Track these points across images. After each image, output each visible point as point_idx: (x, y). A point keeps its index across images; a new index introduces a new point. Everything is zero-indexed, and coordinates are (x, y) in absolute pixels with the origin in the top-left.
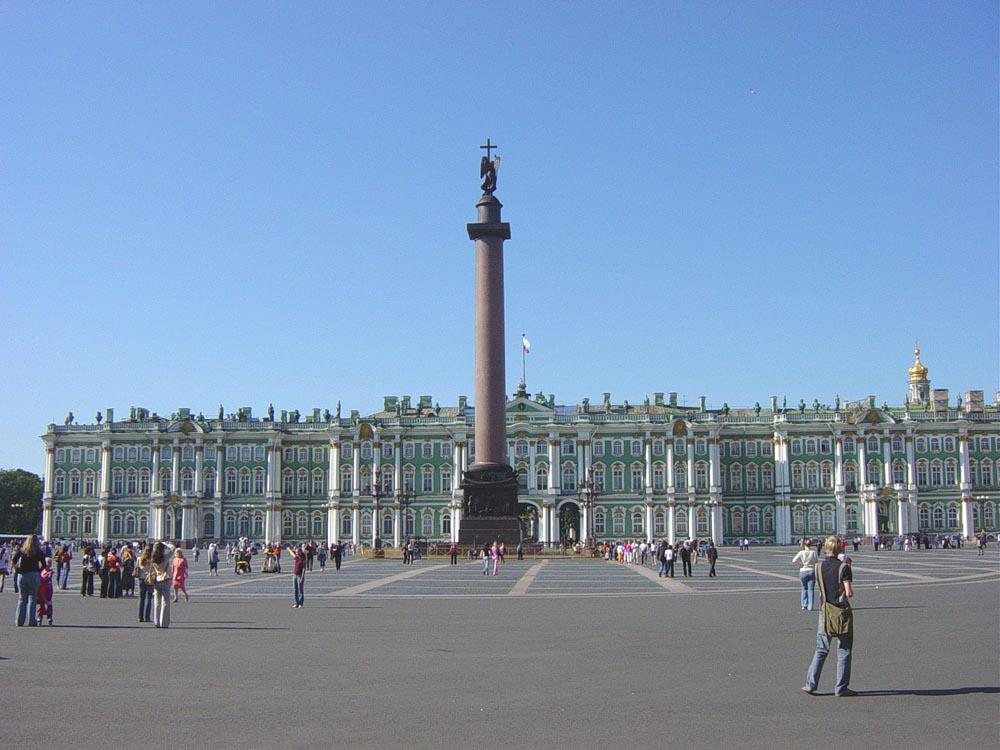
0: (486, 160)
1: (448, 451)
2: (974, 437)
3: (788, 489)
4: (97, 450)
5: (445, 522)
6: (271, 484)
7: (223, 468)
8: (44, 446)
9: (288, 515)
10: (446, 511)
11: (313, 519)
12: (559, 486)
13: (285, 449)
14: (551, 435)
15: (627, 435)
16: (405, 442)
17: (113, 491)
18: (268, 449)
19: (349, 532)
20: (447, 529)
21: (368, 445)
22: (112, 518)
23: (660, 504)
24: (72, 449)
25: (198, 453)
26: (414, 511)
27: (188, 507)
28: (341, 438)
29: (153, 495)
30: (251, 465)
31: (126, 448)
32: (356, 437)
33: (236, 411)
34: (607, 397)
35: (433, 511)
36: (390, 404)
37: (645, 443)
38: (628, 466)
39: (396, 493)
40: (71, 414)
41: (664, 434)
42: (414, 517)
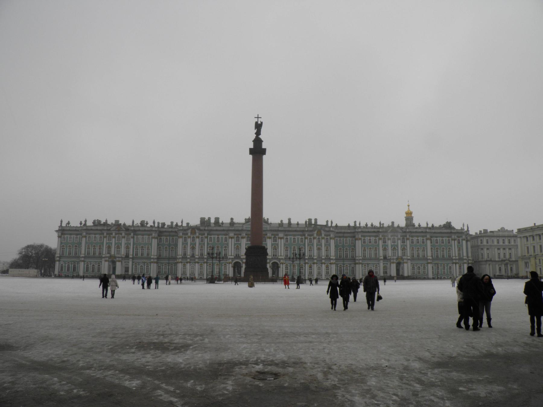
0: (256, 123)
1: (226, 240)
2: (432, 239)
3: (361, 258)
6: (154, 252)
7: (133, 245)
8: (56, 235)
10: (225, 264)
15: (299, 235)
16: (209, 236)
21: (193, 237)
24: (69, 236)
27: (119, 261)
29: (103, 256)
33: (139, 222)
34: (289, 220)
36: (202, 220)
37: (305, 238)
41: (313, 235)
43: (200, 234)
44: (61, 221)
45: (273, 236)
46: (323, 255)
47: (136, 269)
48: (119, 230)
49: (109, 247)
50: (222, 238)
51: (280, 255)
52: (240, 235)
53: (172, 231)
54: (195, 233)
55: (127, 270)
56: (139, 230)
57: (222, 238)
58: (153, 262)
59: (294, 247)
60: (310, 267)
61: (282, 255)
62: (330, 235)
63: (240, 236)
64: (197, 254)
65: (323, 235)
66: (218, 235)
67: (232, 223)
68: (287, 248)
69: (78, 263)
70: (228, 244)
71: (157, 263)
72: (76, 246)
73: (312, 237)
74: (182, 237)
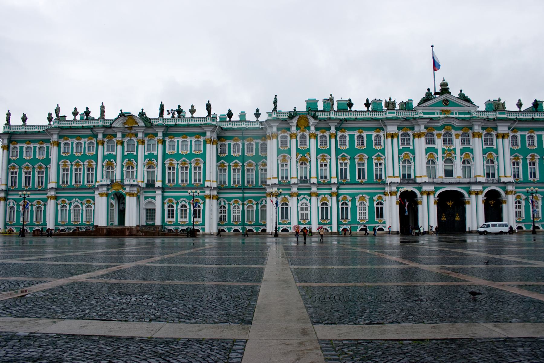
4: (48, 147)
5: (378, 208)
9: (222, 203)
11: (246, 207)
13: (219, 143)
16: (339, 134)
17: (61, 182)
18: (205, 142)
19: (287, 218)
20: (380, 213)
21: (303, 136)
22: (59, 207)
24: (25, 146)
25: (140, 146)
27: (131, 194)
28: (278, 129)
29: (97, 184)
30: (191, 156)
31: (72, 143)
32: (294, 129)
36: (312, 104)
40: (24, 115)
42: (350, 204)
43: (317, 129)
44: (8, 115)
45: (484, 132)
47: (171, 214)
48: (131, 128)
49: (110, 166)
50: (369, 137)
51: (502, 174)
52: (412, 128)
53: (247, 129)
54: (308, 127)
55: (150, 213)
56: (176, 126)
57: (369, 137)
58: (210, 197)
61: (508, 174)
63: (410, 133)
64: (314, 174)
68: (516, 158)
69: (45, 201)
70: (383, 151)
71: (218, 199)
72: (40, 167)
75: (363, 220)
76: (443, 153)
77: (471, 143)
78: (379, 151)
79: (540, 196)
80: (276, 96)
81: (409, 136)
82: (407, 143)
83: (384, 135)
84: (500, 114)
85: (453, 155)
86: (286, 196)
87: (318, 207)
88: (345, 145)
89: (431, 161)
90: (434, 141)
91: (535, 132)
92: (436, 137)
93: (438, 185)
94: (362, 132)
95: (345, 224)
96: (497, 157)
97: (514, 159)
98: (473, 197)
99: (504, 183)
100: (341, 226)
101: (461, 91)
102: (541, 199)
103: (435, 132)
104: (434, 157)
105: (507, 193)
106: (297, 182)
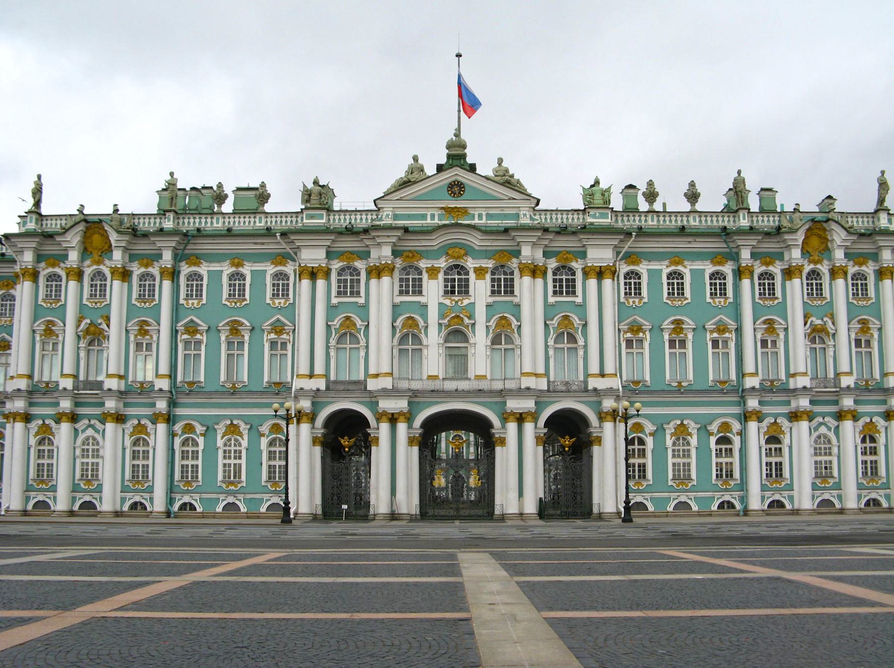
12: (541, 370)
14: (526, 251)
16: (185, 269)
21: (99, 274)
23: (776, 416)
26: (199, 429)
28: (39, 258)
32: (73, 257)
35: (244, 428)
37: (739, 273)
38: (701, 329)
39: (163, 384)
41: (780, 256)
42: (201, 441)
45: (553, 264)
46: (844, 367)
50: (258, 276)
52: (365, 255)
57: (258, 276)
59: (678, 325)
60: (773, 439)
61: (610, 368)
62: (875, 256)
63: (360, 265)
65: (839, 255)
66: (237, 260)
67: (318, 197)
73: (776, 269)
74: (34, 276)
75: (232, 483)
76: (442, 316)
77: (516, 292)
78: (280, 309)
79: (692, 424)
80: (39, 177)
81: (359, 274)
82: (352, 293)
83: (295, 271)
84: (594, 217)
85: (467, 321)
86: (47, 422)
87: (124, 449)
88: (199, 295)
89: (409, 335)
90: (421, 286)
91: (686, 263)
92: (425, 276)
93: (415, 397)
94: (242, 266)
95: (187, 492)
96: (585, 325)
97: (631, 330)
98: (512, 427)
99: (595, 390)
100: (178, 496)
101: (500, 161)
102: (696, 431)
103: (423, 264)
104: (417, 325)
105: (601, 417)
106: (70, 386)
